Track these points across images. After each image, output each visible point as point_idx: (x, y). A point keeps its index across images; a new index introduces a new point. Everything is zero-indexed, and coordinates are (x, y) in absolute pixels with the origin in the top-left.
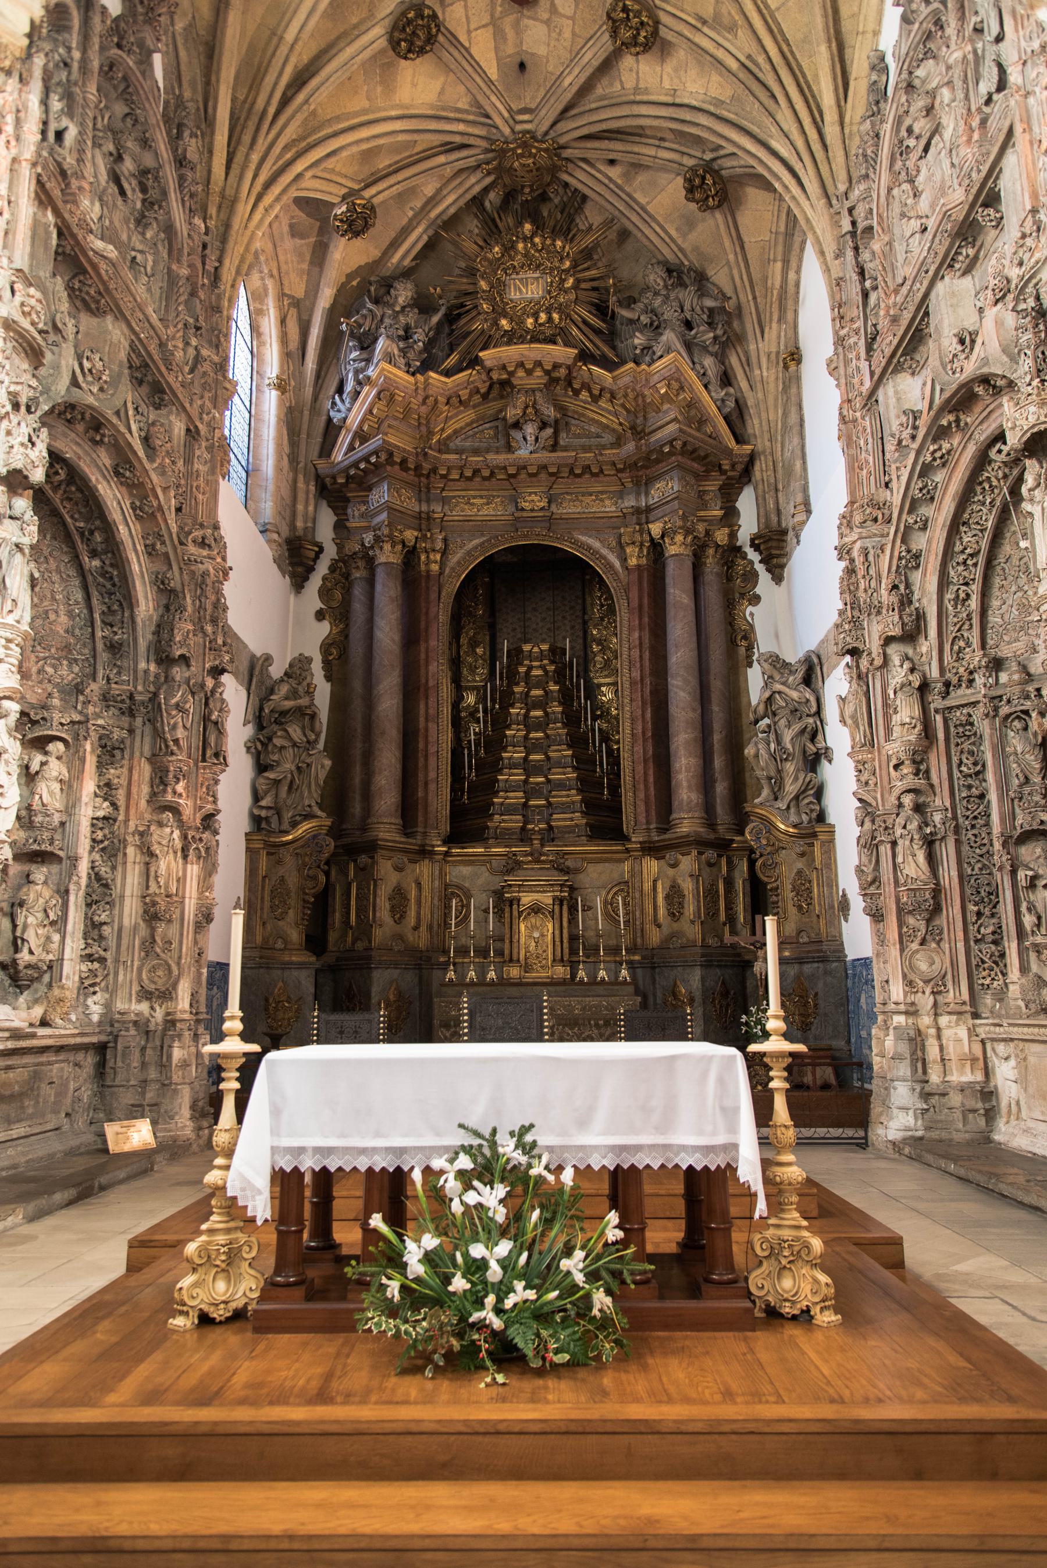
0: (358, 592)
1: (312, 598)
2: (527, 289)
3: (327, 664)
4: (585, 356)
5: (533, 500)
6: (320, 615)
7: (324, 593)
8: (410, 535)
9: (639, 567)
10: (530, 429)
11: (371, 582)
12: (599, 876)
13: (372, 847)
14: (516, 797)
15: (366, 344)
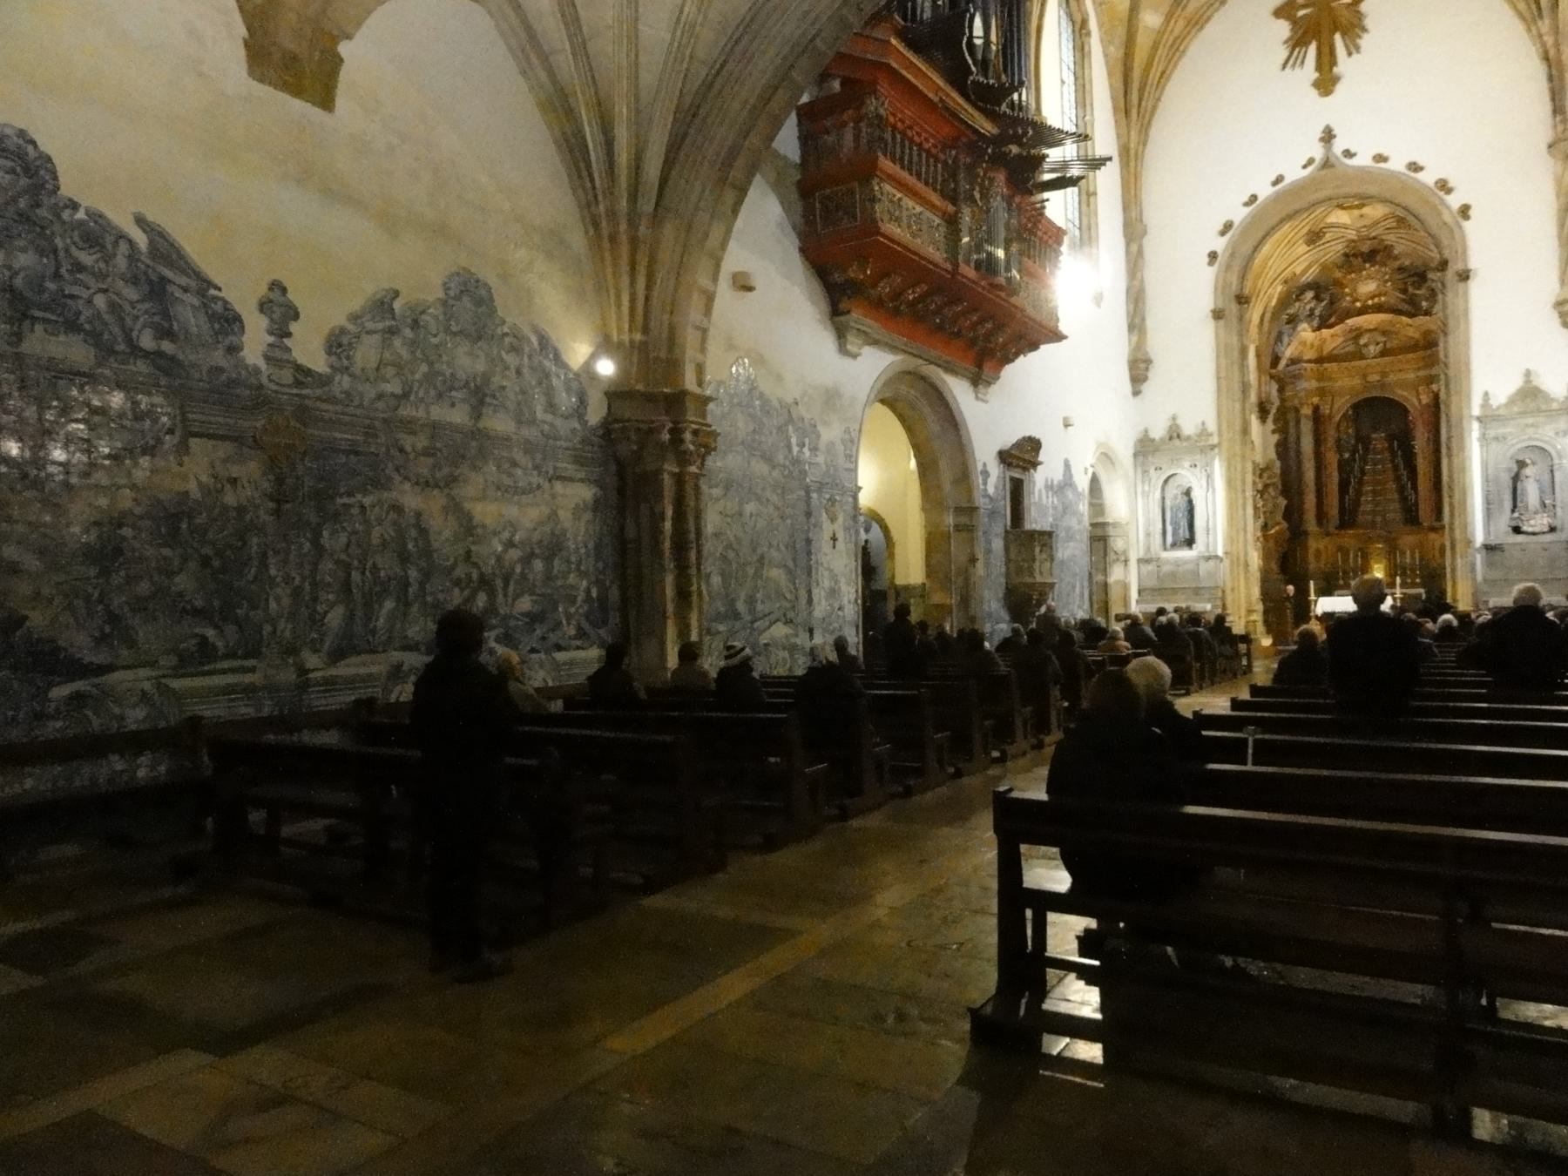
0: (1292, 424)
1: (1270, 425)
2: (1367, 287)
3: (1278, 453)
4: (1399, 312)
5: (1376, 377)
6: (1274, 432)
7: (1275, 421)
8: (1315, 400)
9: (1428, 405)
10: (1372, 348)
11: (1298, 422)
12: (1408, 540)
13: (1306, 533)
14: (1369, 507)
15: (1293, 321)
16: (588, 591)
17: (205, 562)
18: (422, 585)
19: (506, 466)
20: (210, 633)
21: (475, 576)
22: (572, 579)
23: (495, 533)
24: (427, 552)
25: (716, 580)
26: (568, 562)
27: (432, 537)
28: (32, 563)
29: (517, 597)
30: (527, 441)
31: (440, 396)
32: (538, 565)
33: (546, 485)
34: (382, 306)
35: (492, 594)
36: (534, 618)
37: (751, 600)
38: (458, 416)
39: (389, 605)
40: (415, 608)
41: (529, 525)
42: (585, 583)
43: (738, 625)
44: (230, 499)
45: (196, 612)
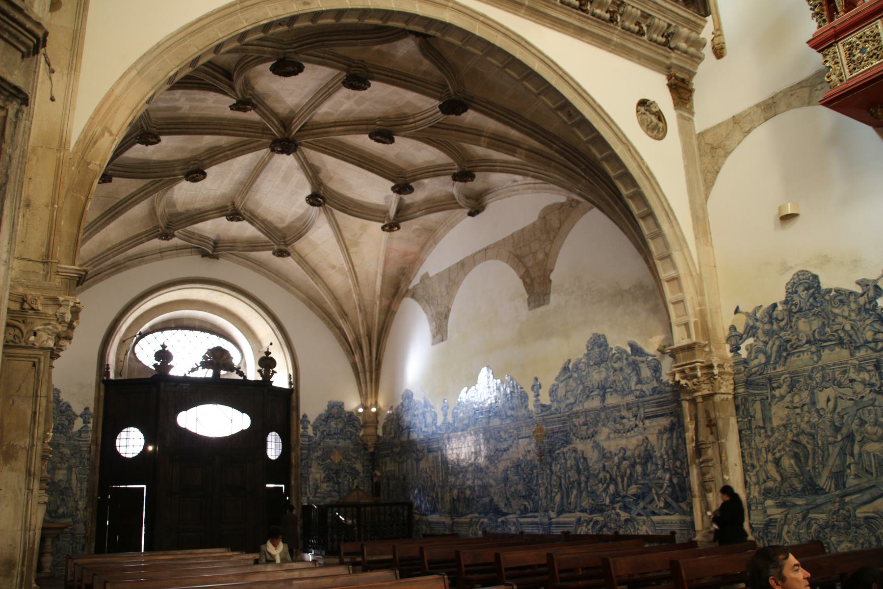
16: (671, 480)
17: (524, 479)
18: (586, 483)
19: (619, 419)
20: (527, 503)
21: (608, 476)
22: (660, 473)
23: (616, 455)
24: (587, 469)
25: (787, 462)
26: (657, 465)
27: (589, 461)
28: (494, 484)
29: (629, 486)
30: (628, 404)
31: (588, 397)
32: (639, 468)
33: (641, 425)
34: (565, 369)
35: (616, 485)
36: (638, 497)
37: (839, 477)
38: (594, 403)
39: (575, 492)
40: (584, 494)
41: (631, 447)
42: (668, 476)
43: (820, 499)
44: (529, 458)
45: (523, 497)
